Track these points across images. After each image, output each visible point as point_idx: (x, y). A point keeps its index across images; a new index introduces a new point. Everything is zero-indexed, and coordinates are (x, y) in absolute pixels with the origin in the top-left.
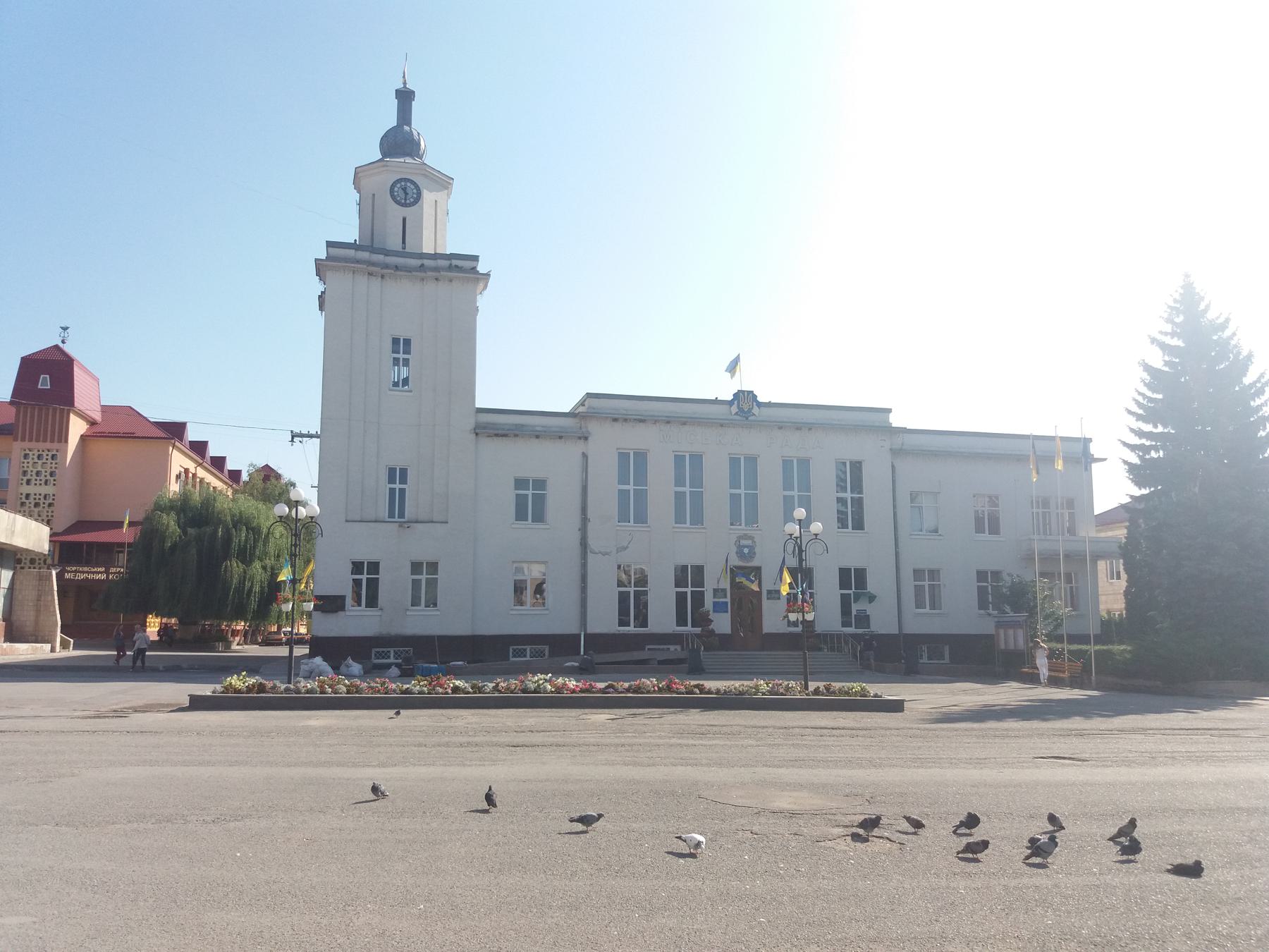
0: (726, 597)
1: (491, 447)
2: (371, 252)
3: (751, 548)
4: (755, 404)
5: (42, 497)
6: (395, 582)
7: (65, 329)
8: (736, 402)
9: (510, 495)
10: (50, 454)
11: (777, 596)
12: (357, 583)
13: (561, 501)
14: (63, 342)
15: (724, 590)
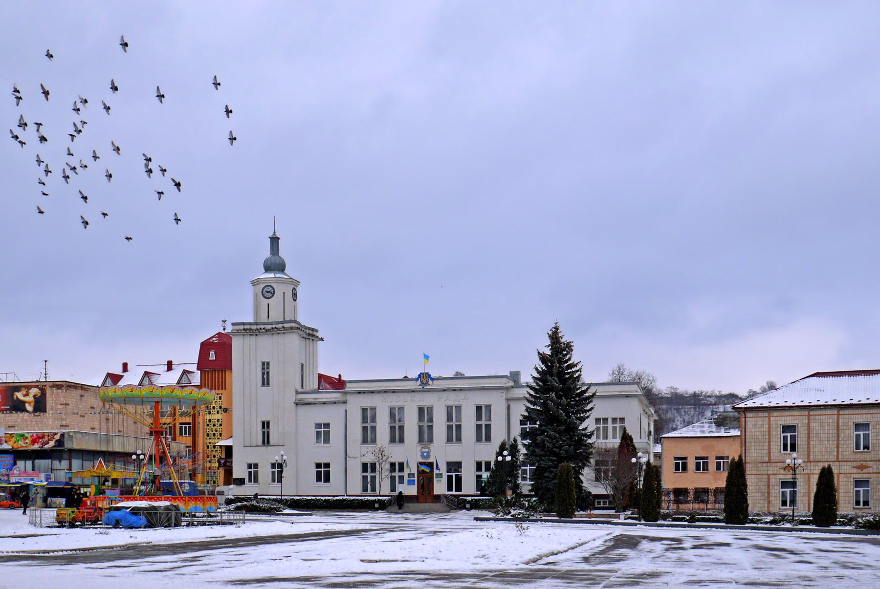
0: (414, 477)
1: (303, 410)
2: (257, 325)
3: (428, 453)
4: (429, 379)
5: (216, 421)
6: (265, 472)
7: (224, 322)
8: (419, 379)
9: (313, 431)
10: (218, 396)
11: (441, 476)
12: (250, 473)
13: (336, 433)
14: (224, 329)
15: (413, 474)
